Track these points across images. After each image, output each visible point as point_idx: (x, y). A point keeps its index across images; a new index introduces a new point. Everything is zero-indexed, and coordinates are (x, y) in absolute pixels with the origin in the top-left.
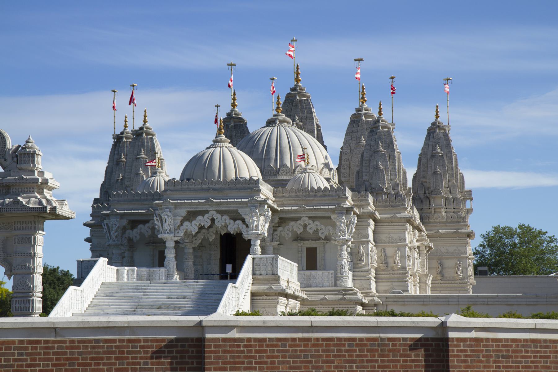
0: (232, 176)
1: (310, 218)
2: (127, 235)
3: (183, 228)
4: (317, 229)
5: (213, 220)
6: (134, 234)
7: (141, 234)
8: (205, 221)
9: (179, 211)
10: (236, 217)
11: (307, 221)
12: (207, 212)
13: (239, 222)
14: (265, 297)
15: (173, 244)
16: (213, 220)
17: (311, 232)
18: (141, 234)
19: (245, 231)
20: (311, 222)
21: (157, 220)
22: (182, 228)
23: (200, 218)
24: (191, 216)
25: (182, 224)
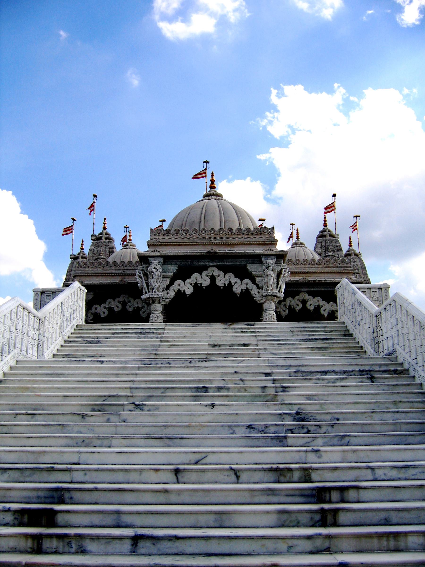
0: (235, 226)
1: (310, 293)
4: (318, 306)
5: (213, 278)
8: (203, 280)
9: (169, 266)
10: (243, 274)
11: (307, 297)
12: (206, 268)
16: (213, 278)
17: (312, 308)
19: (256, 293)
20: (311, 297)
21: (140, 277)
22: (172, 287)
23: (196, 275)
24: (183, 274)
25: (172, 283)
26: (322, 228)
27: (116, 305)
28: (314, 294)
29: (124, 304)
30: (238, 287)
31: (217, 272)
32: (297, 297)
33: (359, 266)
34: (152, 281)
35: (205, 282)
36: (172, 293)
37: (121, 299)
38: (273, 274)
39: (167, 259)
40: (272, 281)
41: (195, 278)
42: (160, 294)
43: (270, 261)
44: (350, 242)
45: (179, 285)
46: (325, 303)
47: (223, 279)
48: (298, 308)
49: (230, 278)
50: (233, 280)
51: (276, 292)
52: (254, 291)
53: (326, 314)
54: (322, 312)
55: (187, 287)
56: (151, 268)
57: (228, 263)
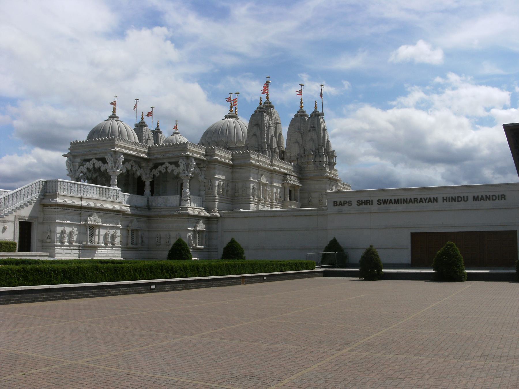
3: (79, 170)
5: (94, 164)
12: (91, 160)
13: (106, 165)
14: (49, 207)
16: (94, 164)
20: (169, 165)
23: (88, 163)
28: (171, 163)
32: (163, 166)
33: (316, 123)
35: (91, 167)
44: (316, 105)
46: (176, 168)
48: (163, 172)
57: (98, 156)
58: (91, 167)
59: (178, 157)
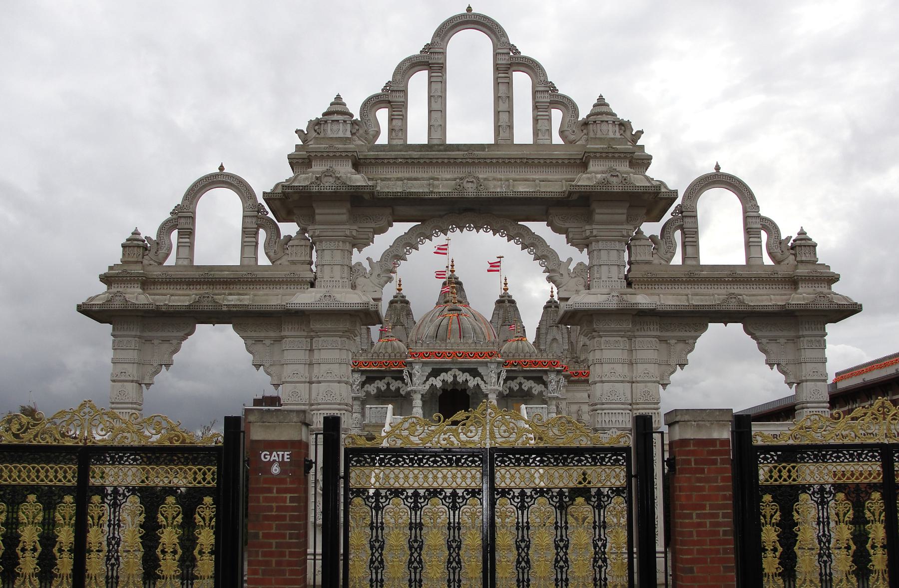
1: (525, 378)
2: (365, 389)
5: (455, 377)
6: (372, 388)
7: (378, 388)
10: (474, 373)
11: (523, 380)
12: (450, 369)
13: (478, 378)
15: (420, 396)
16: (455, 377)
17: (526, 389)
18: (378, 388)
23: (443, 374)
24: (435, 373)
25: (427, 379)
26: (549, 298)
27: (382, 385)
28: (528, 378)
29: (388, 384)
30: (472, 382)
31: (458, 373)
34: (414, 379)
36: (427, 387)
37: (386, 381)
38: (494, 376)
39: (424, 364)
40: (494, 380)
41: (443, 376)
42: (420, 388)
43: (493, 366)
45: (432, 380)
47: (461, 377)
48: (516, 389)
49: (467, 376)
50: (469, 377)
51: (497, 387)
52: (482, 386)
53: (536, 393)
54: (533, 391)
55: (438, 382)
56: (414, 371)
58: (450, 379)
59: (546, 372)
